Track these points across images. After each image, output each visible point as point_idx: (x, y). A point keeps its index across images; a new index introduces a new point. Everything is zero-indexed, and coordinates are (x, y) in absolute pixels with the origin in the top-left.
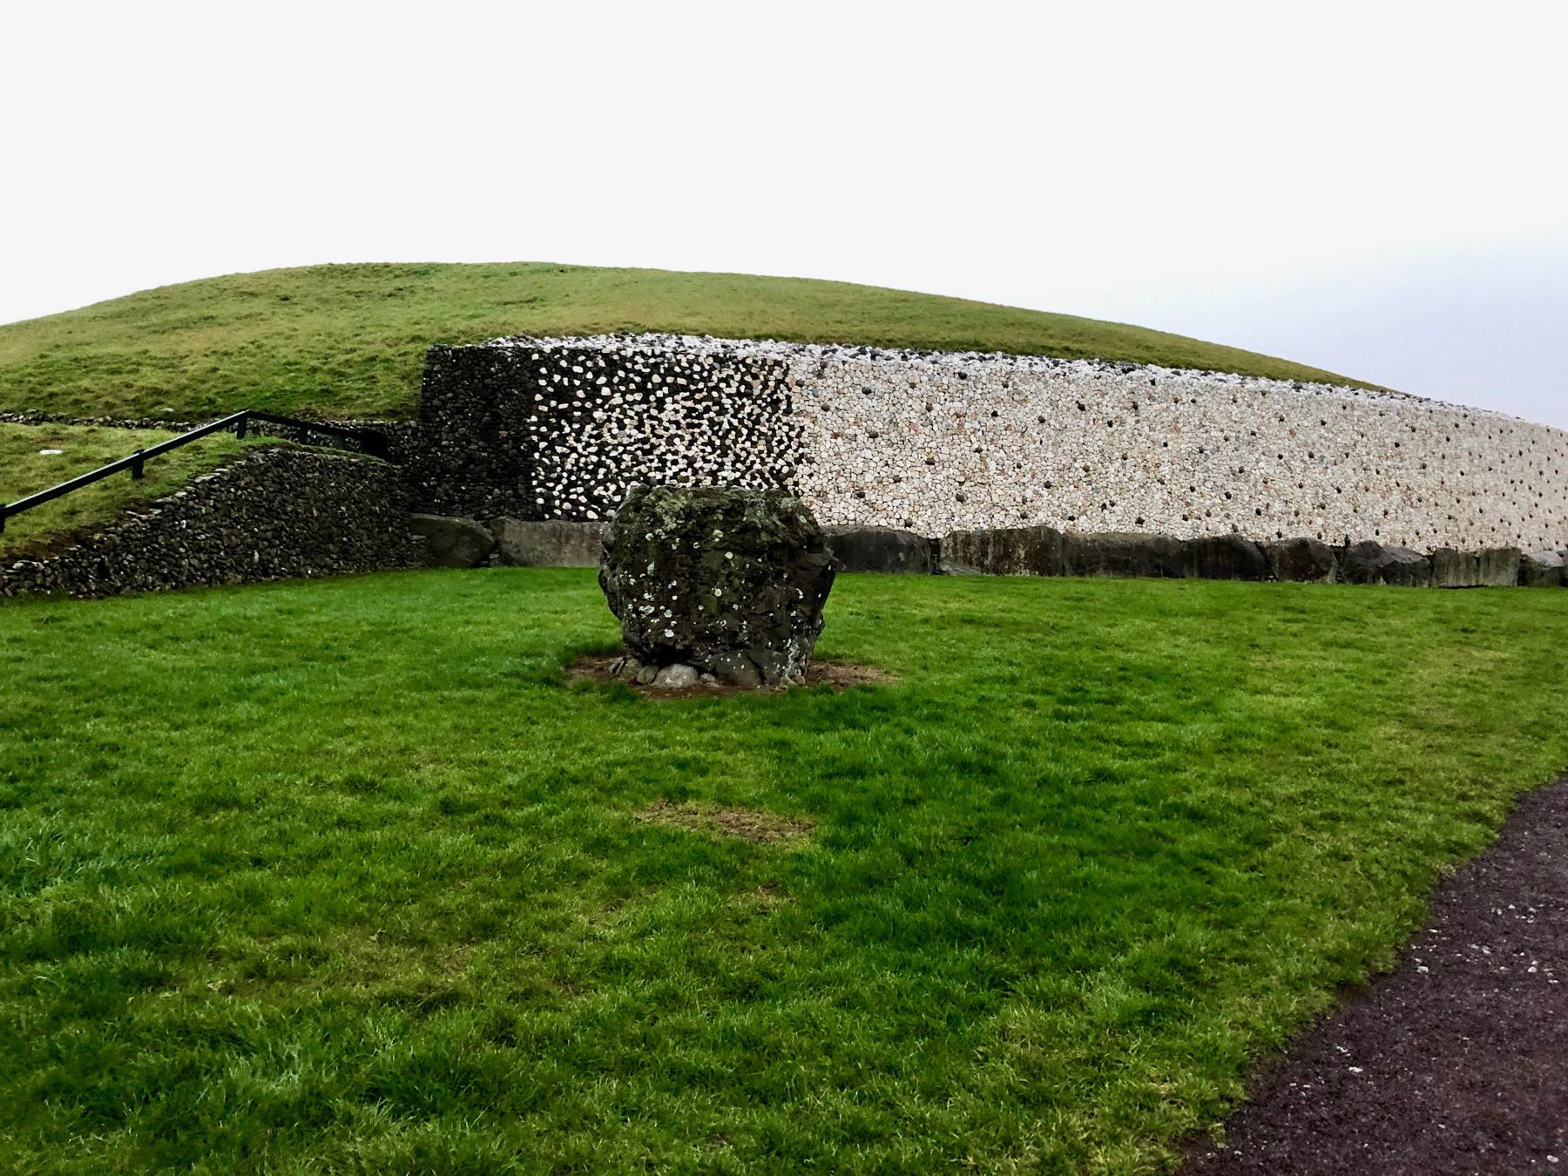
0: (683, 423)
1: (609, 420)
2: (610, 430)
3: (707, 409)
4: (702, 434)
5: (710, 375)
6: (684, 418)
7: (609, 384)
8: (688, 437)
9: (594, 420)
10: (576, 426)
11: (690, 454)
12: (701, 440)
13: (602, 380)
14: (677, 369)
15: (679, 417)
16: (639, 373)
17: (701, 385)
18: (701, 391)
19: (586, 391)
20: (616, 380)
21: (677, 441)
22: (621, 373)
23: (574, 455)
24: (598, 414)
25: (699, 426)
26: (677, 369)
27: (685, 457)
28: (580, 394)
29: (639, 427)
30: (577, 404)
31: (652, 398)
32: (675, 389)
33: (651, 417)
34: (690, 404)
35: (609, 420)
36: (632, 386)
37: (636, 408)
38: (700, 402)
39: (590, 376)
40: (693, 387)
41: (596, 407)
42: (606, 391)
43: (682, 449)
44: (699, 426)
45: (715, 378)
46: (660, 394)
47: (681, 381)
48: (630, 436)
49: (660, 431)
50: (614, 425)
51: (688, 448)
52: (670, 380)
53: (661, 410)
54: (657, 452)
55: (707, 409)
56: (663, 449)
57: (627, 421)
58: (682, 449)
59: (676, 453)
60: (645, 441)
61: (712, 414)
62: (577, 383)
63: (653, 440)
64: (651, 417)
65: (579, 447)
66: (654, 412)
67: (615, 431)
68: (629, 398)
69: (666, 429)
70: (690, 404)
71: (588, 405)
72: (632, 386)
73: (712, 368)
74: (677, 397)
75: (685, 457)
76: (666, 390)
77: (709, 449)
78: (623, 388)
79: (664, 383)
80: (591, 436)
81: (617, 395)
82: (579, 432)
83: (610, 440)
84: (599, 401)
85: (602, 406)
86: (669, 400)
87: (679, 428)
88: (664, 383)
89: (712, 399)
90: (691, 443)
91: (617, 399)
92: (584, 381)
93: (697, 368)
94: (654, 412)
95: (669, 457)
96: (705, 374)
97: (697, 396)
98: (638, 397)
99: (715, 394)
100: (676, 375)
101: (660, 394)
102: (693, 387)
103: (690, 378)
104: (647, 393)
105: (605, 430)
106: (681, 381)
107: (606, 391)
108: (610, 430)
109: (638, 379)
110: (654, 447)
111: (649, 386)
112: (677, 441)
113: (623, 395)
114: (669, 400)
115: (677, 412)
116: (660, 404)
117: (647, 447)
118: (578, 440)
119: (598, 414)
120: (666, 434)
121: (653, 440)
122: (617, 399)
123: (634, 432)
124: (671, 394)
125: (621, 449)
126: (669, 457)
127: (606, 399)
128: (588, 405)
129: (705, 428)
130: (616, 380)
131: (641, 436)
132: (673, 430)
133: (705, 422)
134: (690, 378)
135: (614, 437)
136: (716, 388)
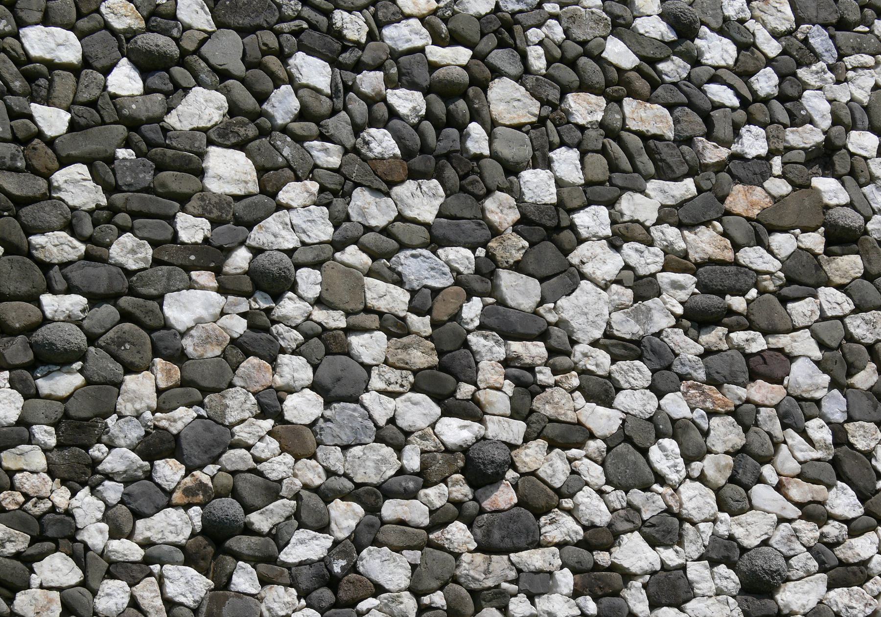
0: (687, 347)
1: (260, 340)
2: (270, 406)
3: (803, 276)
4: (798, 411)
5: (790, 96)
6: (696, 319)
7: (245, 127)
8: (725, 434)
9: (166, 343)
10: (64, 383)
11: (749, 530)
12: (794, 452)
13: (202, 107)
14: (618, 52)
15: (662, 314)
16: (403, 69)
17: (753, 142)
18: (755, 171)
19: (100, 165)
20: (283, 105)
21: (665, 456)
22: (314, 71)
23: (58, 569)
24: (191, 307)
25: (770, 367)
26: (618, 52)
27: (724, 552)
28: (76, 186)
29: (446, 380)
30: (57, 246)
31: (500, 210)
32: (620, 162)
33: (505, 324)
34: (705, 242)
35: (260, 340)
36: (382, 142)
37: (416, 266)
38: (761, 230)
39: (125, 80)
40: (714, 154)
41: (177, 262)
42: (229, 171)
43: (696, 500)
44: (770, 367)
45: (815, 103)
46: (538, 186)
47: (646, 117)
48: (394, 436)
49: (562, 403)
50: (295, 369)
51: (733, 497)
52: (585, 108)
53: (563, 277)
54: (561, 527)
55: (803, 276)
56: (595, 508)
57: (369, 346)
58: (696, 500)
59: (666, 530)
60: (480, 469)
61: (832, 300)
62: (53, 120)
63: (533, 456)
64: (505, 324)
65: (87, 507)
66: (520, 291)
67: (303, 407)
68: (369, 208)
69: (603, 392)
70: (705, 242)
71: (129, 251)
72: (382, 142)
73: (796, 55)
74: (639, 207)
75: (724, 552)
76: (567, 163)
77: (844, 501)
78: (328, 156)
79: (550, 129)
80: (156, 445)
81: (293, 193)
82: (79, 431)
83: (279, 465)
84: (192, 228)
85: (212, 255)
86: (592, 220)
87: (665, 376)
88: (550, 129)
89: (821, 216)
90: (749, 463)
91: (298, 220)
92: (95, 112)
93: (717, 50)
94: (520, 291)
95: (635, 553)
96: (766, 82)
97: (744, 200)
98: (423, 200)
99: (829, 188)
100: (615, 86)
101: (538, 186)
102: (714, 154)
103: (686, 100)
104: (468, 180)
105: (238, 404)
106: (646, 117)
107: (229, 171)
108: (270, 406)
109: (407, 102)
110: (540, 499)
111: (477, 139)
112: (665, 456)
113: (334, 193)
114: (592, 220)
115: (644, 288)
116: (549, 230)
117: (504, 496)
118: (81, 474)
119: (191, 307)
120: (602, 420)
121: (533, 456)
122: (298, 220)
123: (417, 410)
124: (593, 192)
125: (346, 516)
126: (635, 553)
127: (237, 216)
128: (129, 251)
129: (805, 376)
130: (283, 105)
131: (456, 431)
132: (636, 400)
133: (803, 344)
134: (686, 100)
135: (298, 442)
136: (826, 157)
